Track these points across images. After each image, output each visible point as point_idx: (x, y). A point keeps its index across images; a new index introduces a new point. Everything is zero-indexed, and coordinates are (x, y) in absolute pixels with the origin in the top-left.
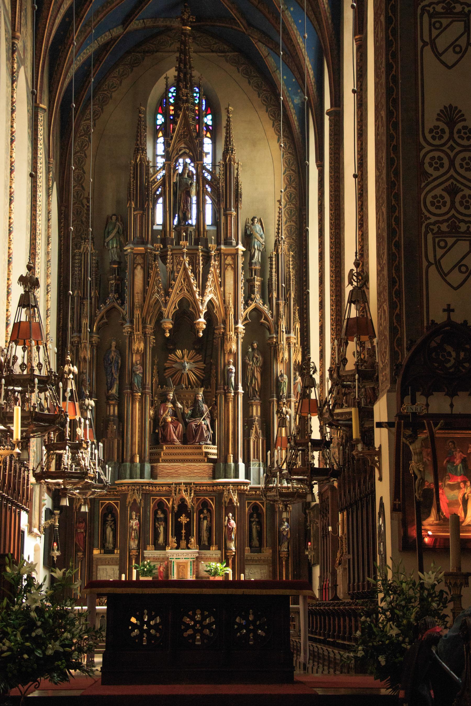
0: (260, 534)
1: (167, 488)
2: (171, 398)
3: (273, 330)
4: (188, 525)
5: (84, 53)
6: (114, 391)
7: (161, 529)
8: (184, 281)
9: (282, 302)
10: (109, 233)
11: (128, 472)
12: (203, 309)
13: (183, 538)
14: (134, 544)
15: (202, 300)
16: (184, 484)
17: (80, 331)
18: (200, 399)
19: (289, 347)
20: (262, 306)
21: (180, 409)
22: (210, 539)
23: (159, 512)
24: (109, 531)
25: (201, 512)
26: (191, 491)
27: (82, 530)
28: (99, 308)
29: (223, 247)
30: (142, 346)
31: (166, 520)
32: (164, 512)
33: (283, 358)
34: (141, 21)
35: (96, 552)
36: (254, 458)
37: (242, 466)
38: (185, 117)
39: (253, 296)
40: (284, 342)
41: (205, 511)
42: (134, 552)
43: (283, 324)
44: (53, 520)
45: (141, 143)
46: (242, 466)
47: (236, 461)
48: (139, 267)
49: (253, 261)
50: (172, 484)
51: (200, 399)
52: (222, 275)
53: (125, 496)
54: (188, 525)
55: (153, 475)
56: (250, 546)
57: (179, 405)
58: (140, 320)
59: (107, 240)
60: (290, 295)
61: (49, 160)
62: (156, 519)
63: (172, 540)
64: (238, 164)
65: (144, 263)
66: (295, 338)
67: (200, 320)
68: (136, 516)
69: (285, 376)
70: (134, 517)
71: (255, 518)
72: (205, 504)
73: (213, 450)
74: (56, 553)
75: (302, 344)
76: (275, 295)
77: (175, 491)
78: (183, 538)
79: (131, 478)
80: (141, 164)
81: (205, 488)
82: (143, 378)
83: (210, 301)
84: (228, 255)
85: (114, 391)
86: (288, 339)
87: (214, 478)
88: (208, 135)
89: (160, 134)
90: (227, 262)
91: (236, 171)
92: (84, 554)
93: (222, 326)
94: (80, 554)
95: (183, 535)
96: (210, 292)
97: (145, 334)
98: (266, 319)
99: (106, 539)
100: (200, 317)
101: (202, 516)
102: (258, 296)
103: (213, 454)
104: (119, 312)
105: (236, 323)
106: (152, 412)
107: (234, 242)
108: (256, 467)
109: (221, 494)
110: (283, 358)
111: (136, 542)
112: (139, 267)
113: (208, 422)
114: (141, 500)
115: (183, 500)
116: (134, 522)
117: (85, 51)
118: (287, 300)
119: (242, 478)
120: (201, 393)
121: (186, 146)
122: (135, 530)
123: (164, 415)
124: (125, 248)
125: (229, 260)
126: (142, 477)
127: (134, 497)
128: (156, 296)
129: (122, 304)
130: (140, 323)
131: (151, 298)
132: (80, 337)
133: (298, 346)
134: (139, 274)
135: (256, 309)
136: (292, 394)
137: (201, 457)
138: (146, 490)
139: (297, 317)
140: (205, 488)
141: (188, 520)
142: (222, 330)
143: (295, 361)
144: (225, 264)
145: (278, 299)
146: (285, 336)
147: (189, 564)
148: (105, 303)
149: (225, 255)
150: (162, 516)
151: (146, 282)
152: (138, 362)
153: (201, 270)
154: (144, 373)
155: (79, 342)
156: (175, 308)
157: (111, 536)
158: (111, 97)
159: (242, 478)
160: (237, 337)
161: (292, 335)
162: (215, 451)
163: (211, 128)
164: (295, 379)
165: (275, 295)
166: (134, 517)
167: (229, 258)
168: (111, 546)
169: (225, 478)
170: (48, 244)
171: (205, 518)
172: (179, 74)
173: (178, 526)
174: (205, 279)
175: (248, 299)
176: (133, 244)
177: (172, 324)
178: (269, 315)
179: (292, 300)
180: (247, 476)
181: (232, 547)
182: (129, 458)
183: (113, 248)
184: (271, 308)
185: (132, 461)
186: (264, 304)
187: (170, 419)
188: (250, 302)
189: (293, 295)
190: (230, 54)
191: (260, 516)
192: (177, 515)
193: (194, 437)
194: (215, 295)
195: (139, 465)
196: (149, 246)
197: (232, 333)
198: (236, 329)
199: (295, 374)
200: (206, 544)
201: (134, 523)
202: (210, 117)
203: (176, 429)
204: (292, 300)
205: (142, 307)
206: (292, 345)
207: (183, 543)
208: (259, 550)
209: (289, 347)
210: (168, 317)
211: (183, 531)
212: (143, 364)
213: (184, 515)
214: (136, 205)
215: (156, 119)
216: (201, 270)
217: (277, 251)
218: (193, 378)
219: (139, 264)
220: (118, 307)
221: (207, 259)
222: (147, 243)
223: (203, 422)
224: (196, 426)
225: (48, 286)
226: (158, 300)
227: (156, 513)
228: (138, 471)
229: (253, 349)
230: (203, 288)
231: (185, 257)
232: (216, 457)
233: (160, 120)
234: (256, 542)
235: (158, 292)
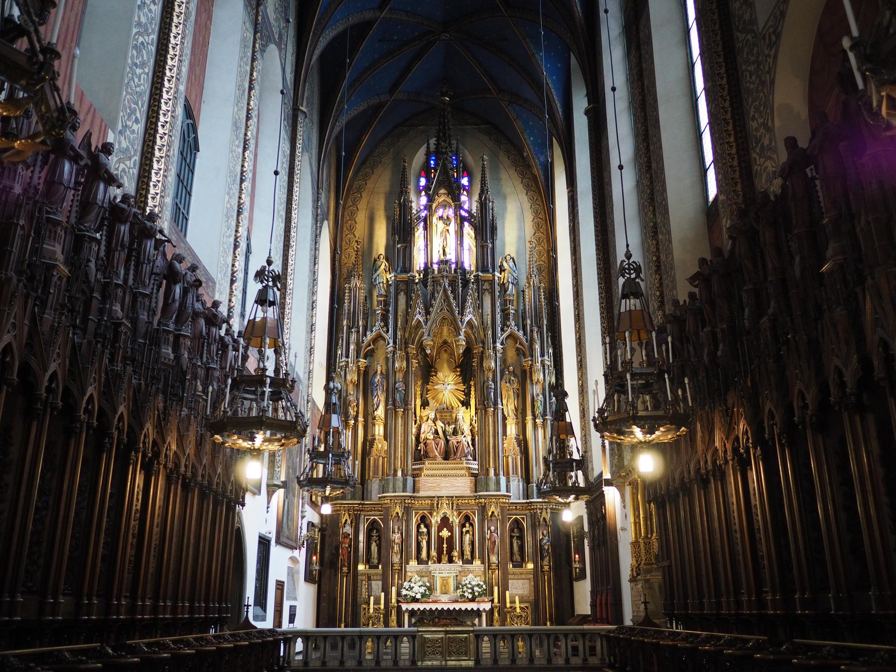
0: (522, 548)
1: (429, 502)
3: (528, 353)
4: (450, 540)
7: (424, 544)
9: (535, 329)
11: (391, 486)
13: (445, 552)
14: (396, 559)
17: (347, 357)
19: (544, 369)
20: (517, 332)
22: (472, 552)
23: (422, 526)
24: (374, 547)
25: (463, 526)
26: (452, 504)
29: (480, 274)
30: (405, 364)
31: (429, 533)
32: (427, 526)
33: (538, 380)
35: (361, 567)
36: (513, 474)
37: (503, 480)
38: (444, 166)
39: (508, 323)
40: (539, 365)
41: (467, 525)
42: (397, 567)
43: (537, 347)
44: (312, 532)
46: (503, 480)
47: (497, 474)
48: (402, 293)
49: (508, 293)
50: (434, 497)
52: (480, 298)
53: (388, 509)
54: (450, 540)
55: (414, 490)
56: (512, 561)
59: (374, 277)
60: (543, 321)
62: (419, 533)
63: (434, 553)
64: (493, 202)
65: (407, 289)
66: (549, 361)
69: (541, 396)
70: (396, 531)
71: (516, 533)
72: (467, 518)
73: (475, 465)
75: (555, 367)
76: (529, 322)
77: (438, 504)
78: (445, 552)
81: (466, 501)
82: (405, 394)
84: (485, 281)
86: (542, 362)
87: (476, 492)
88: (465, 193)
89: (423, 193)
90: (484, 287)
91: (491, 211)
92: (349, 569)
94: (345, 569)
95: (445, 549)
96: (469, 313)
98: (521, 344)
99: (371, 555)
101: (464, 530)
102: (513, 323)
103: (474, 469)
104: (384, 339)
105: (494, 342)
107: (491, 270)
108: (516, 482)
109: (483, 509)
110: (538, 380)
111: (399, 556)
112: (402, 293)
113: (469, 439)
117: (355, 107)
118: (540, 328)
119: (503, 492)
121: (446, 192)
125: (486, 286)
126: (404, 490)
127: (396, 511)
128: (418, 316)
129: (388, 331)
130: (403, 343)
131: (413, 319)
132: (348, 362)
133: (552, 368)
135: (511, 336)
136: (548, 413)
137: (463, 472)
139: (550, 343)
140: (466, 501)
142: (481, 349)
143: (550, 383)
145: (531, 326)
146: (540, 359)
147: (452, 578)
148: (372, 331)
149: (482, 281)
150: (425, 530)
151: (408, 305)
152: (401, 380)
153: (460, 291)
157: (376, 550)
158: (381, 162)
159: (503, 492)
160: (496, 355)
161: (546, 357)
162: (477, 467)
164: (550, 399)
165: (529, 322)
166: (396, 531)
167: (486, 284)
168: (376, 561)
169: (486, 491)
171: (467, 532)
173: (440, 539)
174: (464, 301)
175: (504, 325)
178: (524, 340)
179: (545, 327)
180: (508, 490)
181: (494, 559)
184: (525, 334)
186: (518, 331)
187: (432, 437)
188: (506, 329)
189: (545, 322)
190: (483, 127)
191: (521, 530)
192: (440, 529)
193: (455, 454)
195: (401, 479)
197: (491, 351)
198: (494, 348)
199: (550, 393)
200: (470, 558)
201: (396, 537)
203: (437, 445)
204: (545, 327)
205: (404, 329)
206: (546, 367)
207: (445, 558)
208: (519, 565)
209: (544, 369)
211: (445, 546)
213: (445, 529)
214: (399, 238)
215: (419, 181)
216: (460, 291)
217: (529, 284)
220: (384, 335)
223: (464, 439)
224: (458, 443)
225: (313, 302)
226: (420, 321)
227: (418, 527)
229: (509, 372)
233: (423, 182)
234: (517, 557)
235: (420, 313)
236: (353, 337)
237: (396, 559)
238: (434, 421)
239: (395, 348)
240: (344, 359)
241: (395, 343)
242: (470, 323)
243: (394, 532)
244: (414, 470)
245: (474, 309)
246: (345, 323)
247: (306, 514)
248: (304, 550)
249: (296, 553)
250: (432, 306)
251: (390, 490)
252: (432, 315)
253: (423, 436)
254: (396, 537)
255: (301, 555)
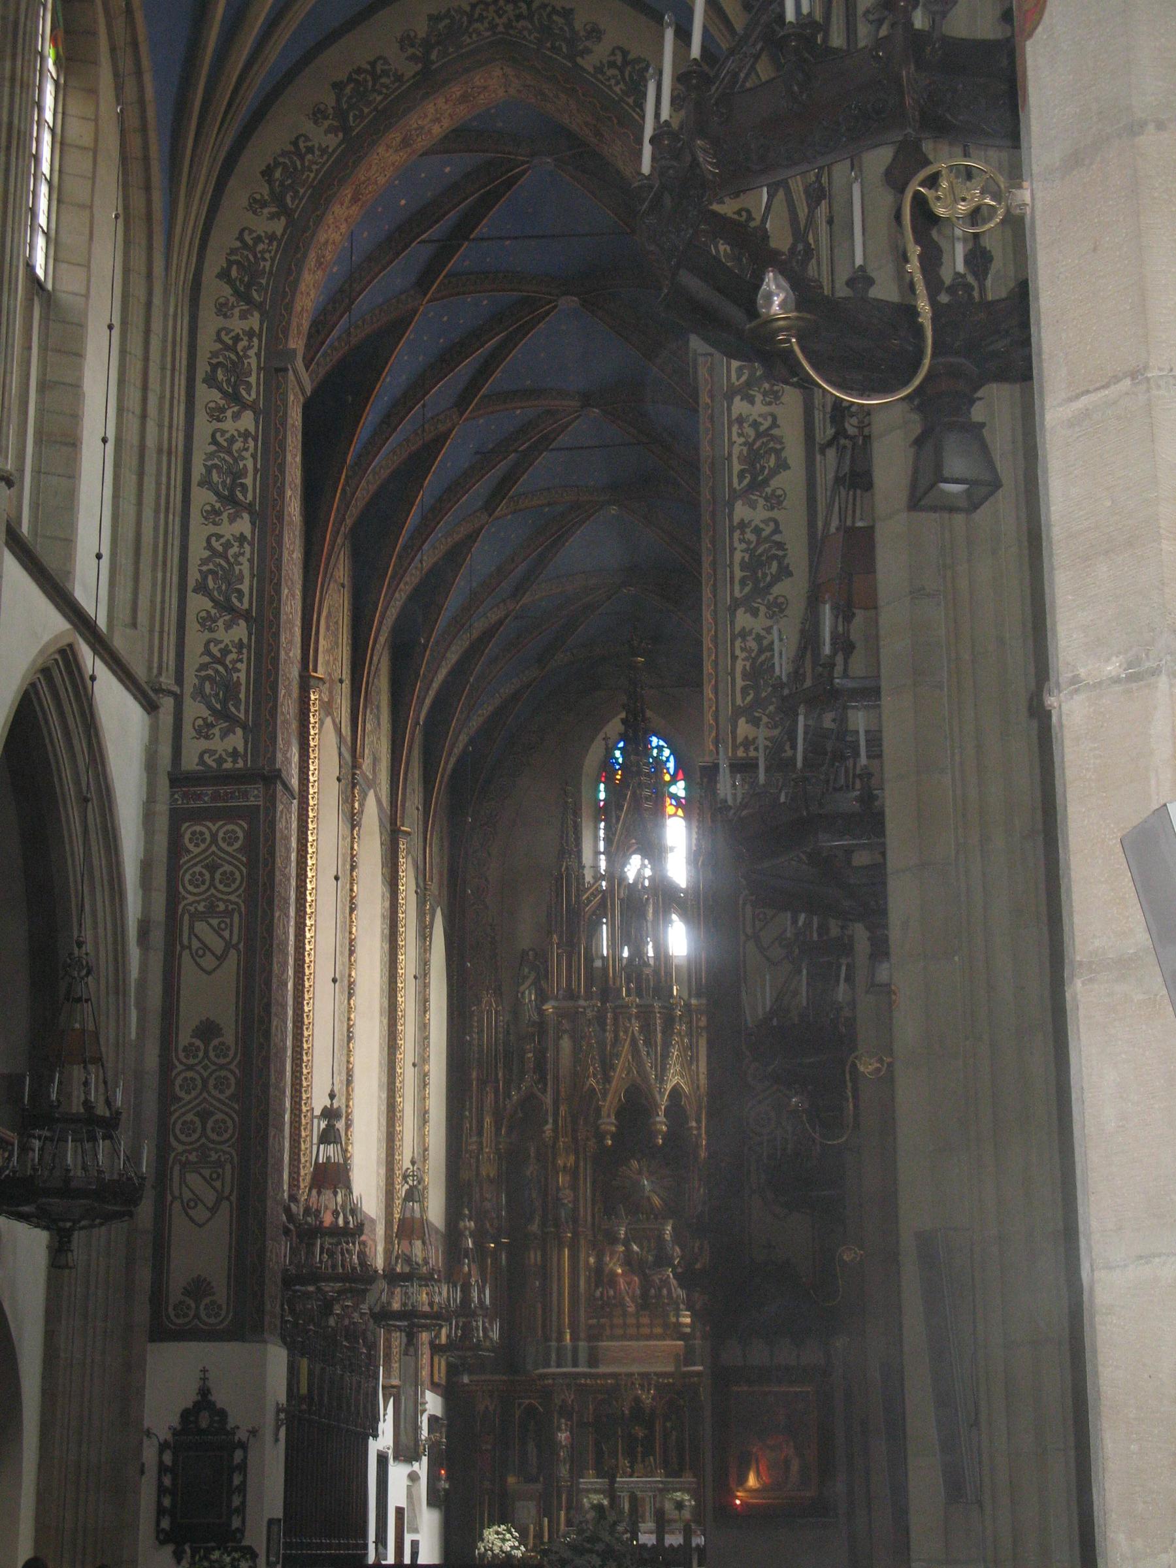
2: (622, 1236)
5: (479, 716)
6: (534, 1227)
8: (633, 1058)
10: (525, 978)
12: (664, 1102)
13: (639, 1459)
14: (564, 1471)
15: (660, 1089)
16: (639, 1374)
17: (480, 1133)
18: (668, 1237)
21: (637, 1253)
27: (489, 1447)
28: (509, 1096)
30: (572, 1158)
34: (568, 653)
35: (511, 1480)
45: (567, 843)
51: (668, 1237)
57: (635, 1248)
58: (569, 1119)
61: (425, 884)
67: (658, 1119)
68: (566, 1425)
70: (563, 1427)
74: (444, 1485)
78: (639, 1459)
79: (558, 1366)
80: (568, 875)
83: (675, 1086)
85: (534, 1227)
88: (680, 812)
93: (694, 1124)
97: (575, 1140)
100: (658, 1115)
103: (686, 1325)
106: (592, 1260)
114: (572, 1401)
115: (637, 1399)
116: (564, 1435)
120: (669, 1228)
122: (566, 1446)
123: (611, 1265)
124: (544, 1008)
126: (575, 1365)
128: (592, 1081)
129: (544, 1091)
132: (481, 1143)
134: (566, 1043)
138: (581, 1385)
141: (646, 1432)
142: (695, 1132)
144: (698, 1027)
148: (520, 1088)
152: (567, 1185)
154: (576, 1200)
155: (481, 1149)
156: (620, 1100)
163: (683, 801)
170: (425, 1012)
172: (626, 731)
174: (665, 1056)
176: (556, 999)
177: (616, 1126)
182: (554, 1335)
183: (530, 1001)
185: (560, 1338)
194: (682, 1077)
196: (582, 1002)
202: (681, 784)
210: (609, 1116)
212: (574, 1187)
214: (560, 937)
218: (656, 1201)
219: (565, 1031)
221: (669, 1021)
222: (578, 997)
228: (569, 1355)
230: (664, 1069)
231: (633, 1021)
232: (688, 1330)
235: (595, 1076)
236: (490, 1099)
237: (564, 1471)
238: (626, 1244)
239: (555, 1130)
240: (474, 1139)
241: (555, 1122)
242: (676, 1092)
243: (560, 1430)
244: (590, 1327)
245: (682, 1066)
246: (474, 1075)
247: (427, 1406)
248: (425, 1459)
249: (416, 1465)
250: (613, 1067)
251: (553, 1363)
252: (614, 1083)
253: (607, 1271)
254: (563, 1437)
255: (422, 1467)
